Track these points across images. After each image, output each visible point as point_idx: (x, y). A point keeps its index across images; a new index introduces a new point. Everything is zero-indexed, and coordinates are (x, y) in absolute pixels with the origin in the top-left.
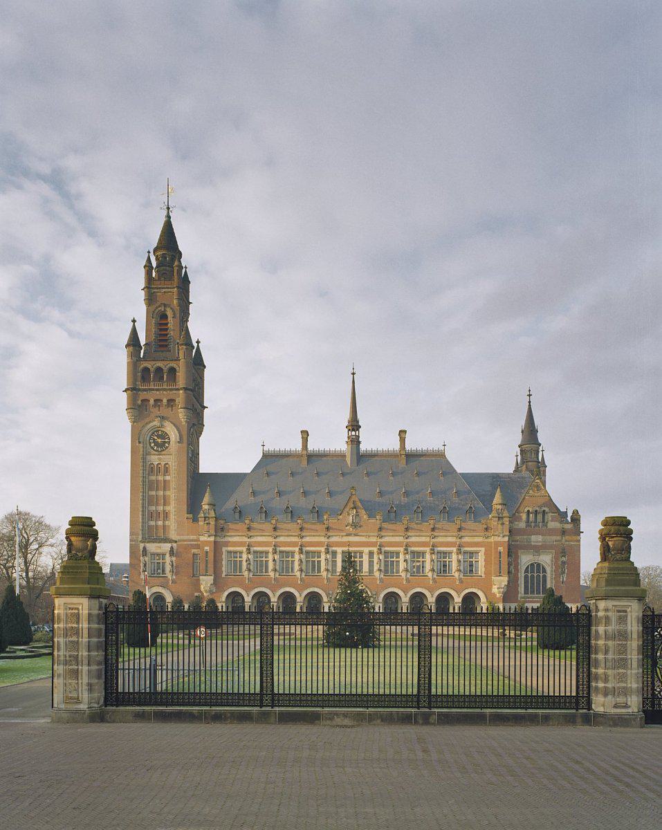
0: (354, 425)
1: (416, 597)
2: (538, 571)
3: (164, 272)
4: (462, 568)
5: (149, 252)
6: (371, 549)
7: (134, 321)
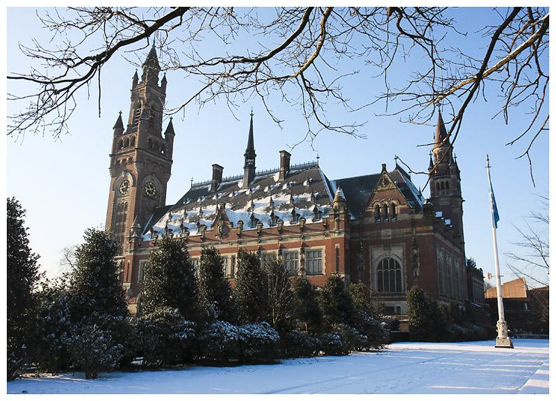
0: (250, 154)
2: (392, 267)
4: (305, 267)
6: (233, 254)
7: (121, 113)
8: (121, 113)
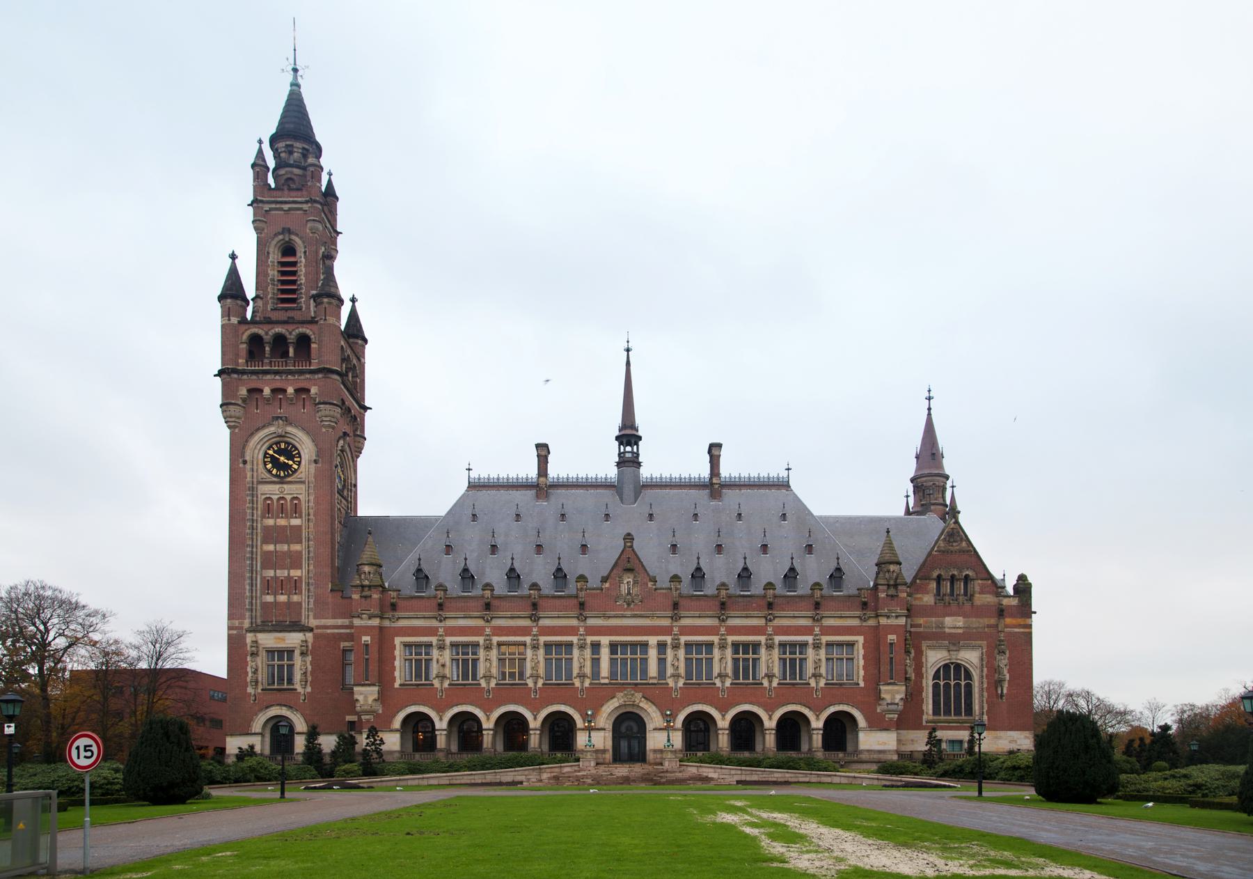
1: (742, 719)
3: (289, 176)
5: (260, 142)
7: (233, 257)
8: (233, 257)
